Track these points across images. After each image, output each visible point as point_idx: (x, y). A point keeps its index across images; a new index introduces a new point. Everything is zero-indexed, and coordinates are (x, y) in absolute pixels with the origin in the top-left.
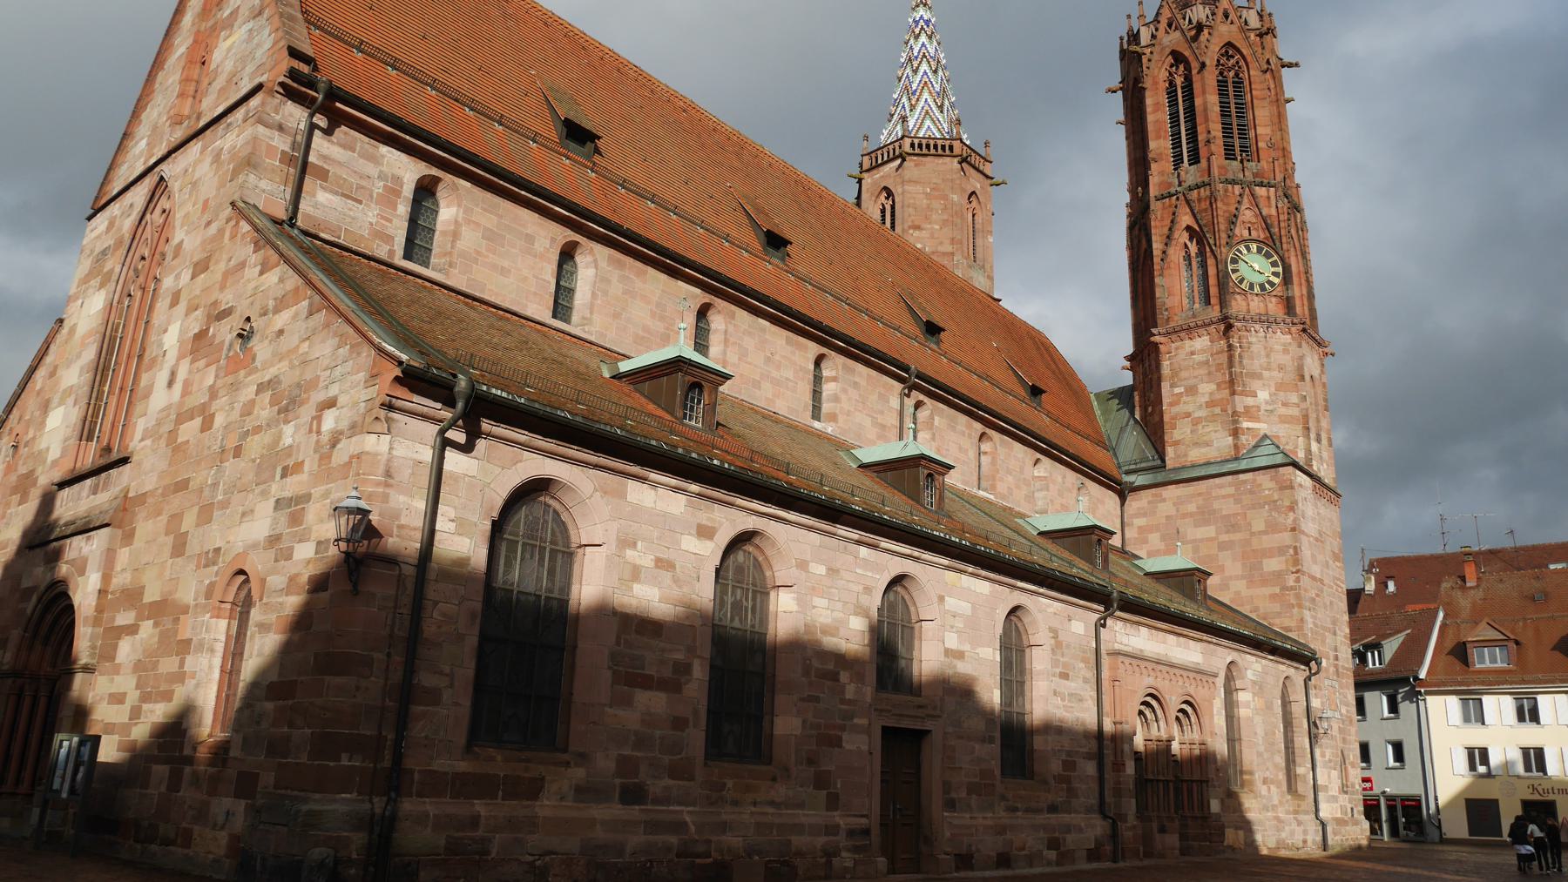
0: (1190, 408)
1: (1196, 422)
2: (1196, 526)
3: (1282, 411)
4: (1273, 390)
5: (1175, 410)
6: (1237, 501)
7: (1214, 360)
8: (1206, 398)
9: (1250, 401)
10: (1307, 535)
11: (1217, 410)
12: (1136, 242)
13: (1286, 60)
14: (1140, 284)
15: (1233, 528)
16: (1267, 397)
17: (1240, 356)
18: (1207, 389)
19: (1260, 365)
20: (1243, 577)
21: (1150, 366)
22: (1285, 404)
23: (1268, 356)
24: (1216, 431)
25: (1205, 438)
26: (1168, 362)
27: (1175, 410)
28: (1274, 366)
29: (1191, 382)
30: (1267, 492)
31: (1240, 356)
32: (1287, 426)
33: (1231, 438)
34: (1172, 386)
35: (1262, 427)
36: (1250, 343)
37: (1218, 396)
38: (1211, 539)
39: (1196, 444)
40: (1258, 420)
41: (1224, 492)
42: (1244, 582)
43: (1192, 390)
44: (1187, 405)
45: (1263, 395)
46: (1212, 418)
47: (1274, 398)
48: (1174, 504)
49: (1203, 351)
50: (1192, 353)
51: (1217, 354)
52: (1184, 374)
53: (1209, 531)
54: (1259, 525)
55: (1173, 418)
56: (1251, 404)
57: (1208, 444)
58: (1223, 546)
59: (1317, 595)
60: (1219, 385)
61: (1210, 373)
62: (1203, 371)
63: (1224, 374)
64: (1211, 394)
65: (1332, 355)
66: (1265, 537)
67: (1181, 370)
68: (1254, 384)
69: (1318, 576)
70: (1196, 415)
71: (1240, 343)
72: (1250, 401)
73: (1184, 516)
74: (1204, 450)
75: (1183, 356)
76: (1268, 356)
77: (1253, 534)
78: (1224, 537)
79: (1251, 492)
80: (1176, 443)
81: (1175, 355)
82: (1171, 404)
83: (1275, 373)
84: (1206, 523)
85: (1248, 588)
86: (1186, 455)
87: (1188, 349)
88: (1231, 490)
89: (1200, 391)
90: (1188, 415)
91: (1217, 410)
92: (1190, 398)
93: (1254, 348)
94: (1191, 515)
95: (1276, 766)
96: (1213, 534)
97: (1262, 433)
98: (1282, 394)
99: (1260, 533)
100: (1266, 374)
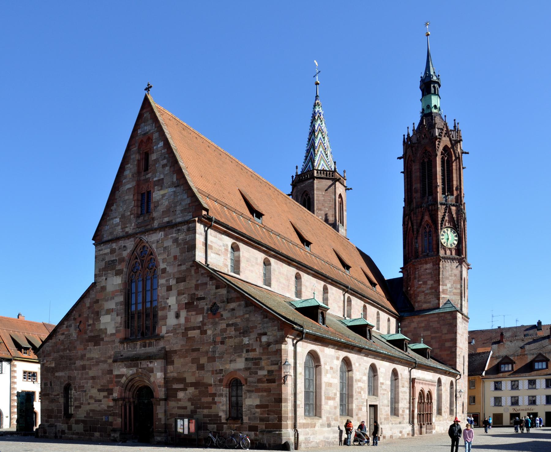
0: (424, 289)
1: (426, 295)
2: (424, 331)
3: (455, 291)
4: (452, 283)
5: (419, 290)
6: (438, 323)
7: (433, 272)
8: (429, 286)
9: (445, 288)
10: (459, 334)
11: (433, 291)
12: (406, 223)
13: (464, 151)
14: (407, 240)
15: (437, 332)
16: (450, 286)
17: (443, 271)
18: (430, 283)
19: (449, 274)
20: (439, 348)
21: (410, 272)
22: (455, 289)
23: (451, 271)
24: (432, 298)
25: (429, 300)
26: (417, 272)
27: (419, 290)
28: (453, 275)
29: (425, 280)
30: (448, 320)
31: (443, 271)
32: (456, 296)
33: (437, 301)
34: (419, 281)
35: (448, 297)
36: (446, 266)
37: (434, 286)
38: (429, 336)
39: (425, 302)
40: (446, 294)
41: (434, 320)
42: (439, 350)
43: (425, 283)
44: (424, 288)
45: (449, 285)
46: (431, 294)
47: (452, 286)
48: (417, 323)
49: (430, 269)
50: (426, 269)
51: (435, 270)
52: (422, 277)
53: (428, 333)
54: (445, 331)
55: (418, 293)
56: (445, 288)
57: (429, 302)
58: (432, 338)
59: (461, 353)
60: (434, 282)
61: (432, 277)
62: (429, 276)
63: (437, 278)
64: (432, 285)
65: (471, 269)
66: (447, 335)
67: (422, 275)
68: (447, 282)
69: (461, 347)
70: (426, 292)
71: (443, 266)
72: (445, 288)
73: (420, 327)
74: (428, 305)
75: (423, 270)
76: (451, 271)
77: (443, 334)
78: (433, 335)
79: (443, 320)
80: (419, 302)
81: (420, 270)
82: (417, 288)
83: (453, 278)
84: (428, 330)
85: (440, 352)
86: (422, 306)
87: (425, 268)
88: (437, 319)
89: (428, 283)
90: (423, 292)
91: (433, 291)
92: (424, 286)
93: (447, 268)
94: (423, 327)
95: (447, 407)
96: (430, 334)
97: (448, 298)
98: (455, 285)
99: (446, 334)
100: (450, 278)
